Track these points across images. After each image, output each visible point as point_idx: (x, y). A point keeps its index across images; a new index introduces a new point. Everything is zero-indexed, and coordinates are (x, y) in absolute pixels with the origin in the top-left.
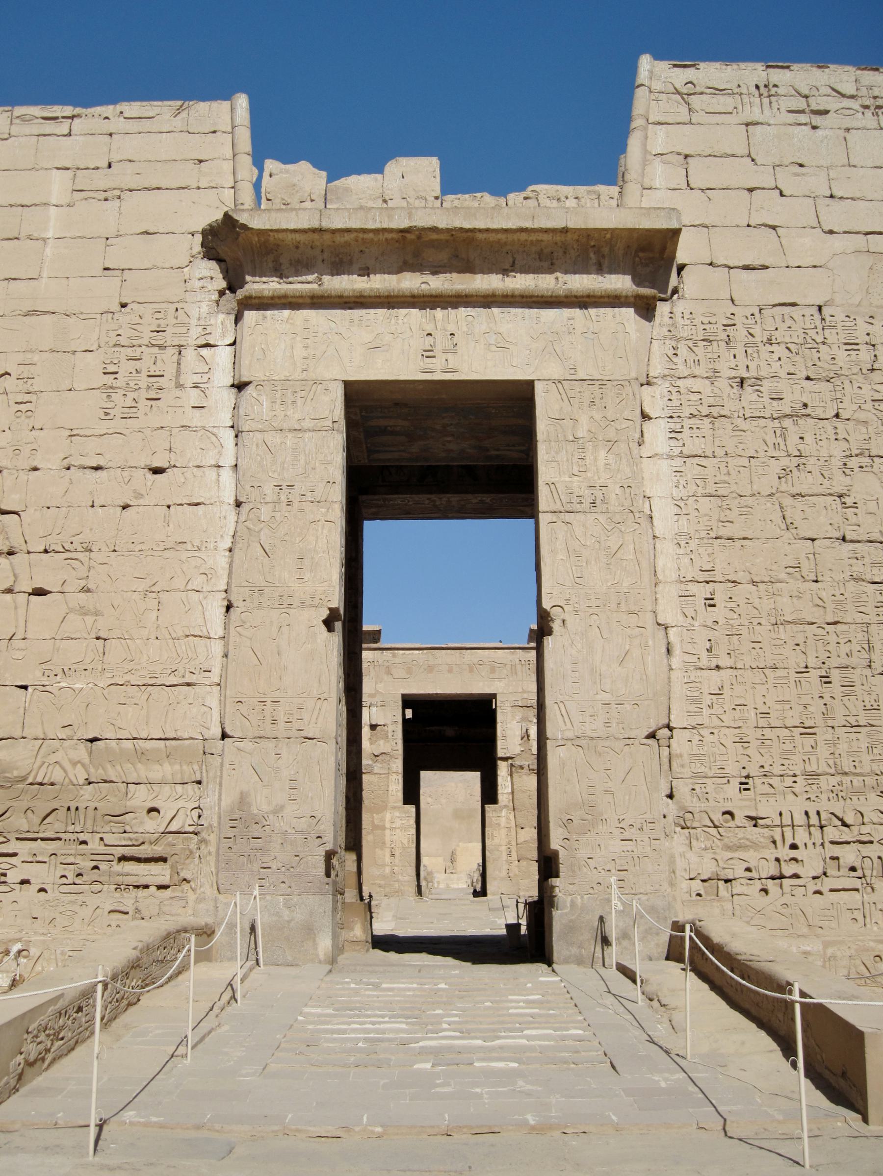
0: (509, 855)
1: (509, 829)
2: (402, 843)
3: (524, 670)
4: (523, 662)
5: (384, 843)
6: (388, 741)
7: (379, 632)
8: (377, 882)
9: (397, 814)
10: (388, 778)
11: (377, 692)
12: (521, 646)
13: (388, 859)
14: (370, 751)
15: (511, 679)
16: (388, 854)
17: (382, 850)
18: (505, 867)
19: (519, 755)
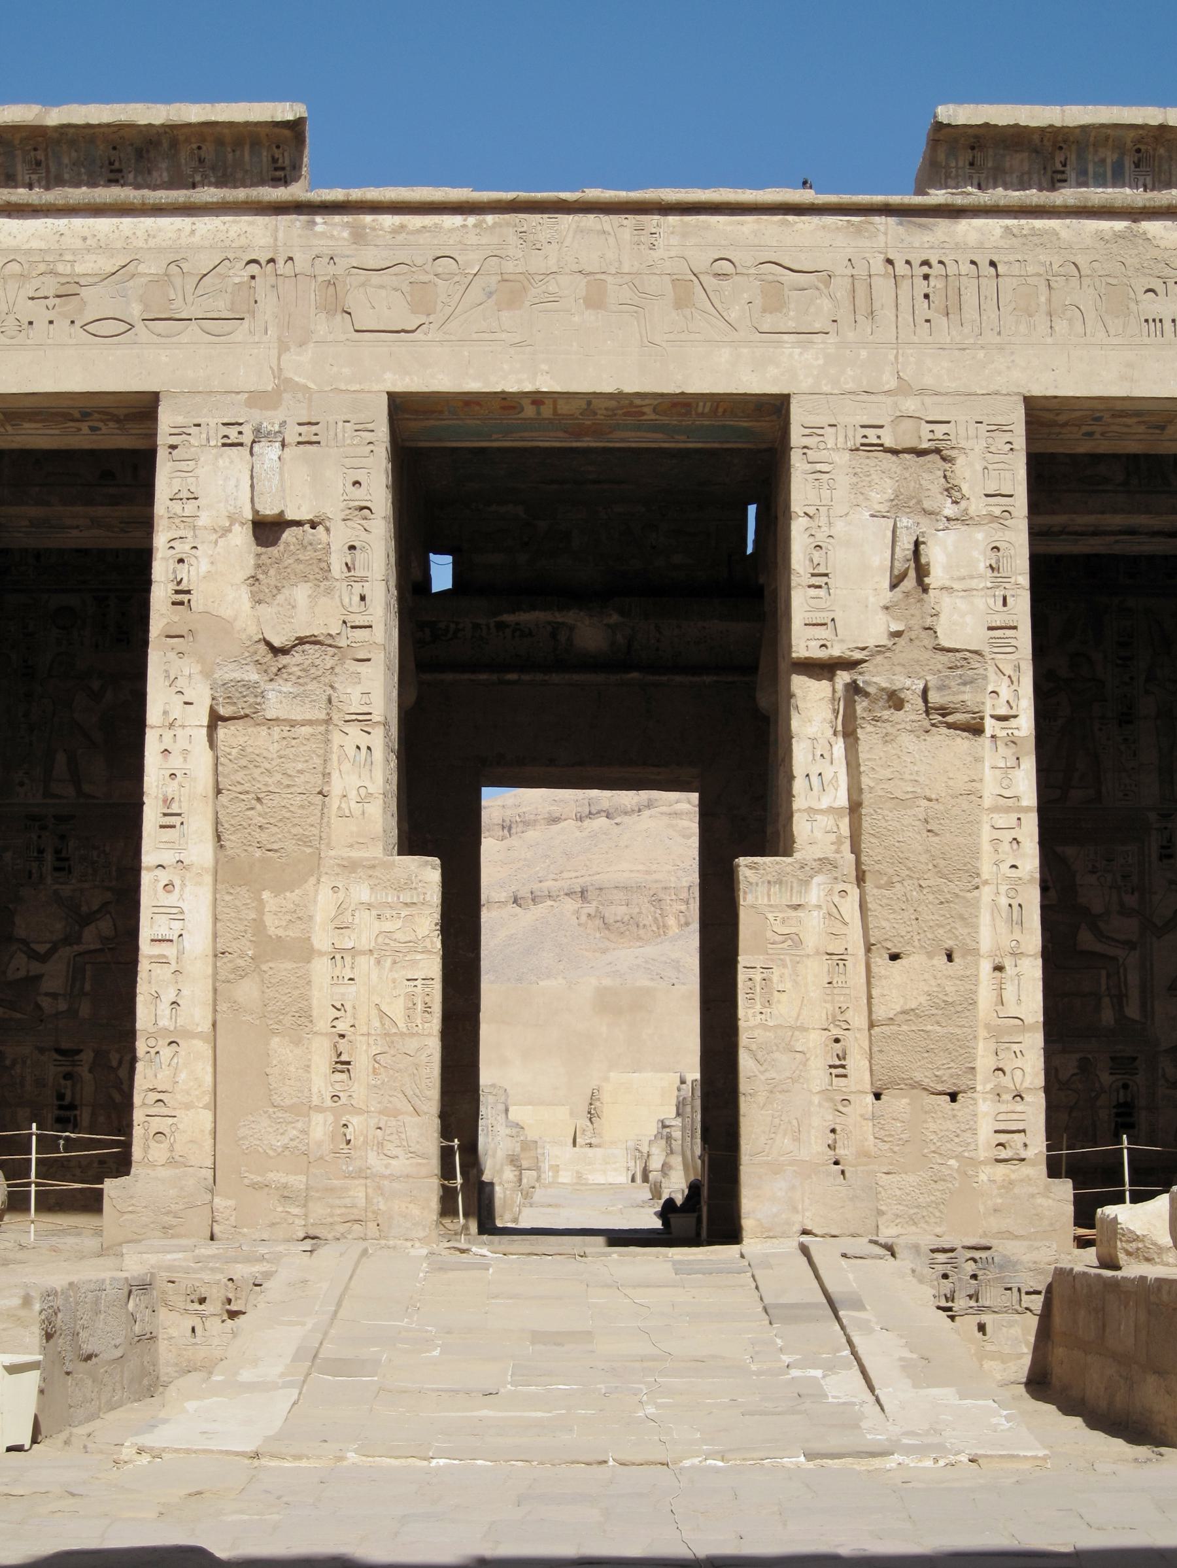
0: (839, 1068)
1: (839, 959)
2: (382, 1014)
3: (905, 302)
4: (901, 268)
5: (306, 1015)
6: (329, 591)
7: (296, 127)
8: (277, 1177)
9: (362, 892)
10: (327, 741)
11: (284, 386)
12: (895, 199)
13: (321, 1081)
14: (253, 631)
15: (851, 336)
16: (322, 1060)
17: (297, 1042)
18: (822, 1118)
19: (881, 650)
